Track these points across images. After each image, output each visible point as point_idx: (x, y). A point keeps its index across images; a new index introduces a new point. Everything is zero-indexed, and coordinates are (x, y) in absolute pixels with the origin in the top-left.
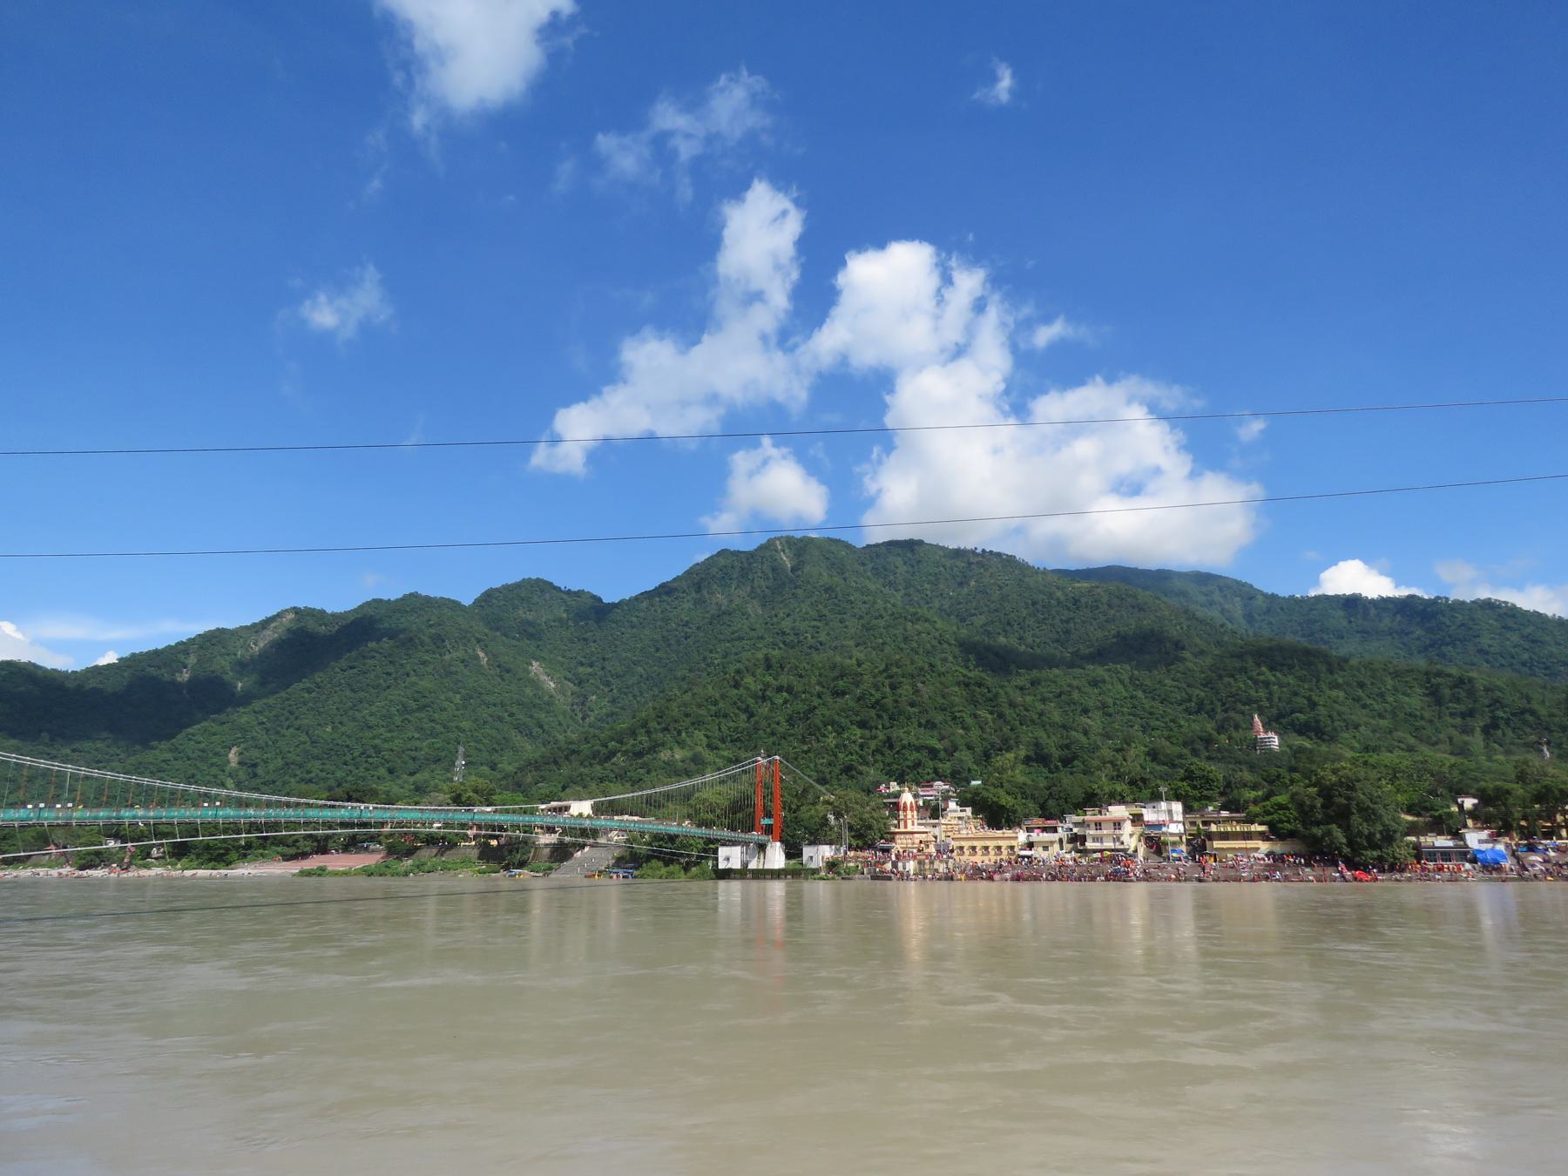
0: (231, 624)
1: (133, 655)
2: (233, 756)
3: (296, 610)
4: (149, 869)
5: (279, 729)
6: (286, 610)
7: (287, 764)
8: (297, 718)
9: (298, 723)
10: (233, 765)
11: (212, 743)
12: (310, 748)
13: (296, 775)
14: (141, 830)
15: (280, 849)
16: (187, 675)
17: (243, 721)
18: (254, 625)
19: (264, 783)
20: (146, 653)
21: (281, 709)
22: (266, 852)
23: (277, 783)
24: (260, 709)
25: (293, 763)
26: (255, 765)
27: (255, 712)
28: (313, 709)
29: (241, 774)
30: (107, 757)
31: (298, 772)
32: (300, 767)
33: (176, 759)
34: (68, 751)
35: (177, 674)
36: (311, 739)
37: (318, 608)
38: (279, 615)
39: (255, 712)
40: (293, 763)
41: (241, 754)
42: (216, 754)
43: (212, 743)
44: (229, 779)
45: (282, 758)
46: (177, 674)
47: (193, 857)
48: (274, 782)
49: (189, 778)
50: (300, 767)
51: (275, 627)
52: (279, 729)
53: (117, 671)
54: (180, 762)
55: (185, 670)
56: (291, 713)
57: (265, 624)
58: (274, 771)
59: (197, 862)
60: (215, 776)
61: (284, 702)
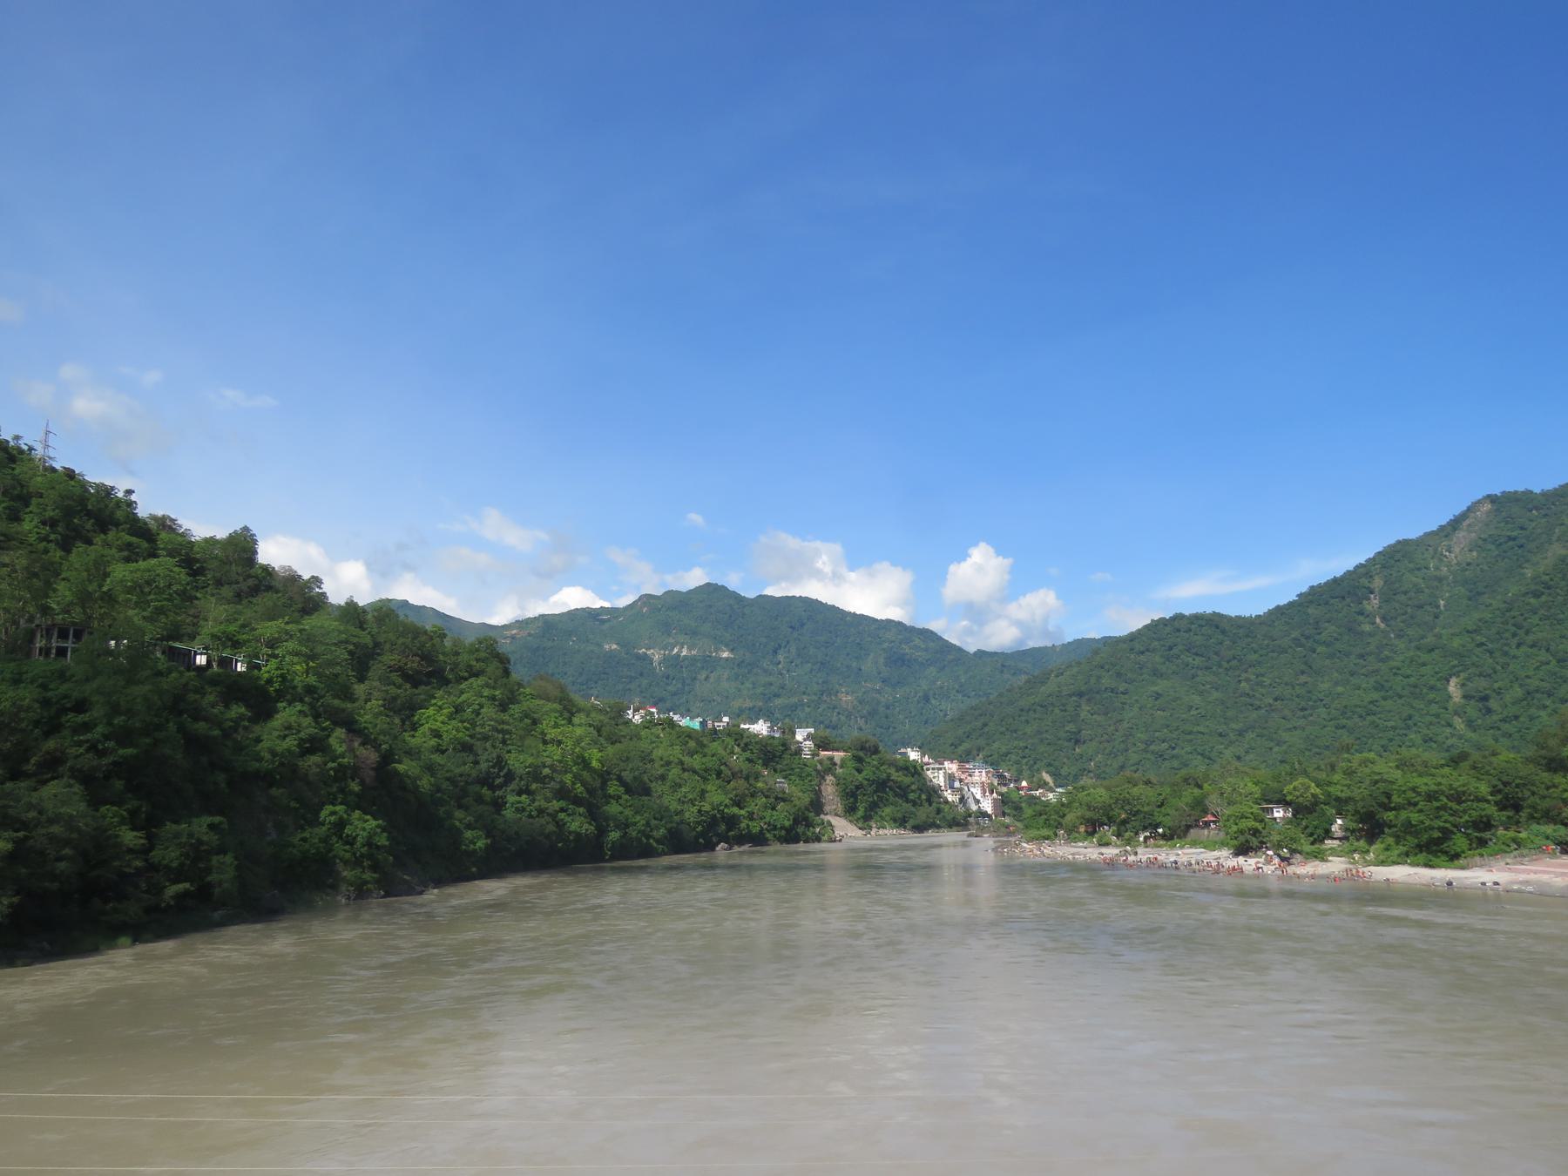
0: (1413, 533)
1: (1312, 588)
2: (1453, 688)
3: (1492, 499)
4: (1324, 860)
5: (1506, 648)
6: (1479, 502)
7: (1529, 693)
8: (1527, 632)
9: (1530, 638)
10: (1457, 700)
11: (1423, 676)
12: (1557, 669)
13: (1545, 707)
14: (1313, 795)
15: (1549, 829)
16: (1376, 601)
17: (1455, 645)
18: (1442, 528)
19: (1503, 721)
20: (1325, 583)
21: (1502, 623)
22: (1523, 835)
23: (1522, 719)
24: (1475, 627)
25: (1537, 691)
26: (1485, 699)
27: (1468, 632)
28: (1547, 618)
29: (1472, 710)
30: (1311, 703)
31: (1548, 703)
32: (1549, 696)
33: (1385, 699)
34: (1271, 701)
35: (1365, 602)
36: (1552, 655)
37: (1521, 489)
38: (1470, 510)
39: (1468, 632)
40: (1537, 691)
41: (1463, 685)
42: (1432, 688)
43: (1423, 676)
44: (1455, 717)
45: (1521, 686)
46: (1365, 602)
47: (1391, 840)
48: (1516, 718)
49: (1405, 720)
50: (1549, 696)
51: (1469, 525)
52: (1506, 648)
53: (1299, 608)
54: (1390, 702)
55: (1372, 596)
56: (1519, 627)
57: (1455, 523)
58: (1513, 704)
59: (1397, 852)
60: (1437, 716)
61: (1503, 614)
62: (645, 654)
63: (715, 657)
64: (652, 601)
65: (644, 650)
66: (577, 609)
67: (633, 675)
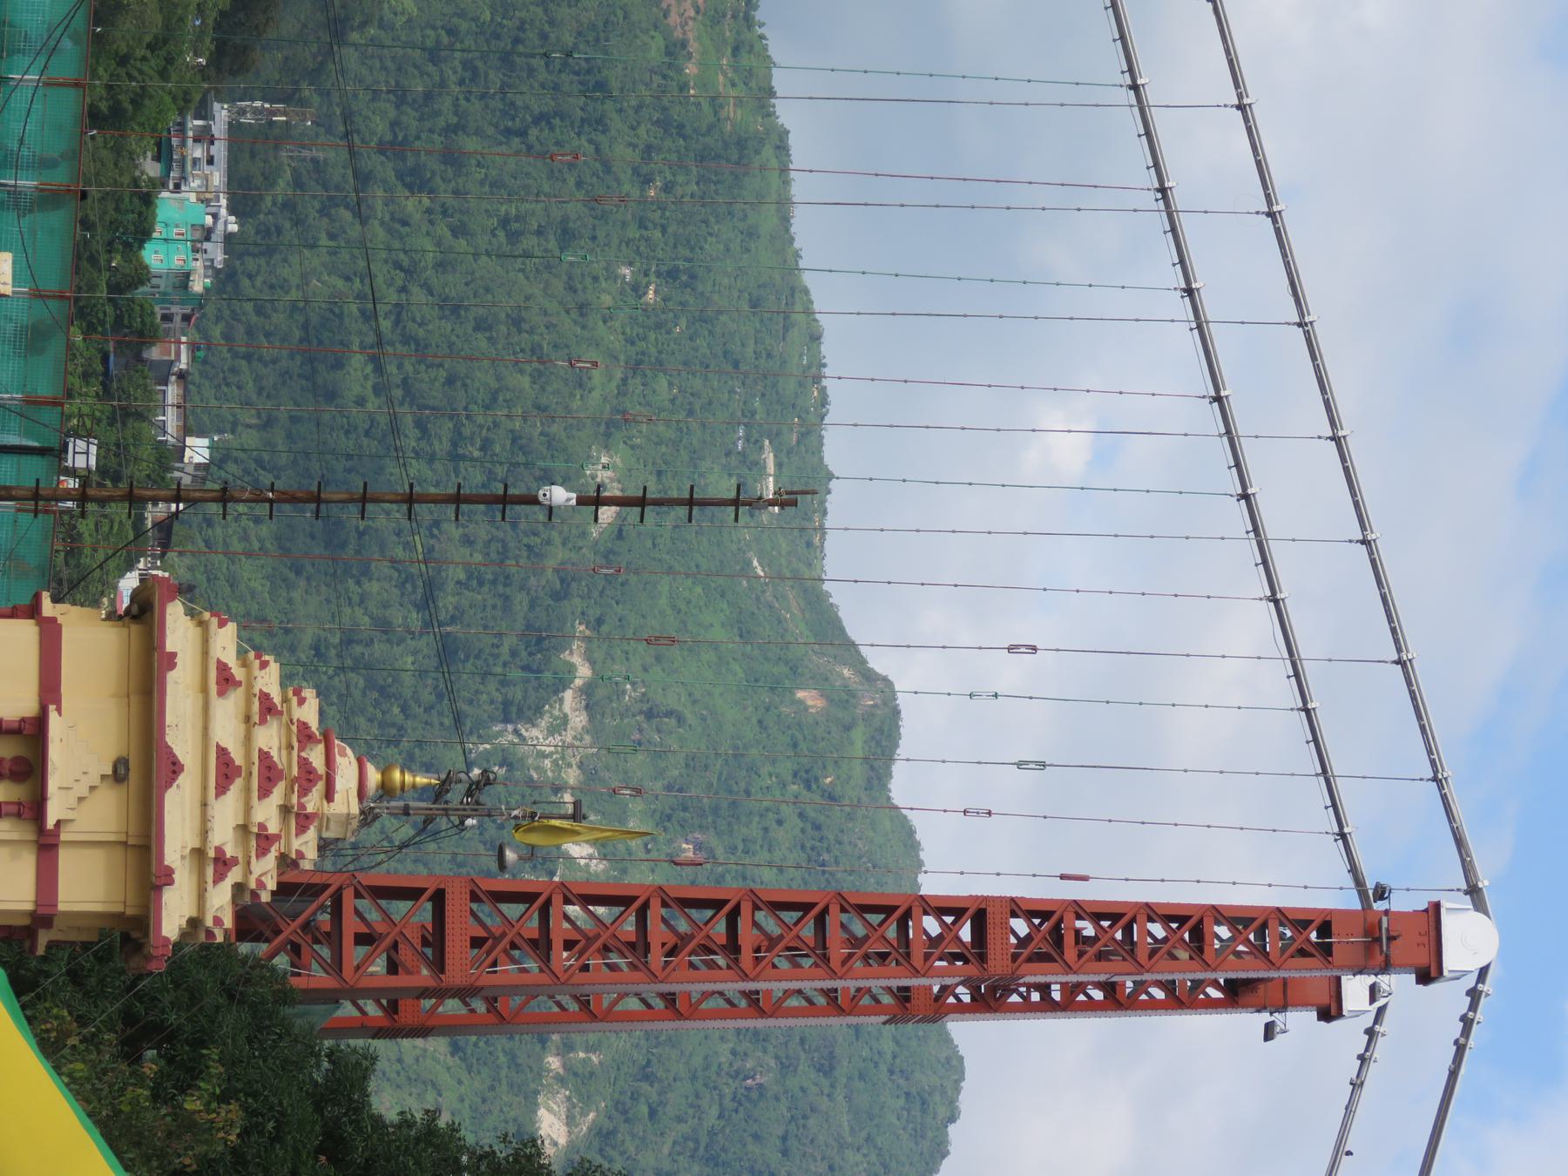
62: (561, 684)
63: (541, 1071)
64: (858, 735)
65: (584, 672)
66: (815, 338)
67: (447, 602)
